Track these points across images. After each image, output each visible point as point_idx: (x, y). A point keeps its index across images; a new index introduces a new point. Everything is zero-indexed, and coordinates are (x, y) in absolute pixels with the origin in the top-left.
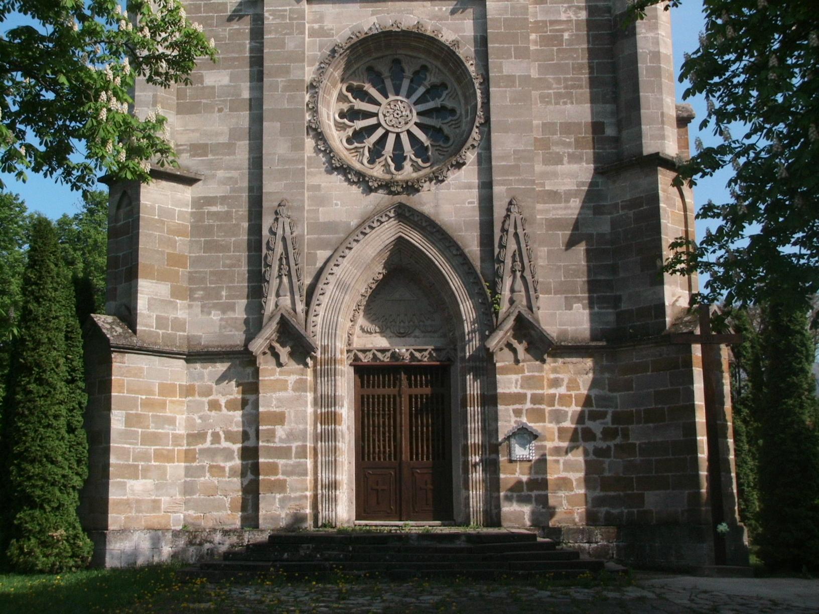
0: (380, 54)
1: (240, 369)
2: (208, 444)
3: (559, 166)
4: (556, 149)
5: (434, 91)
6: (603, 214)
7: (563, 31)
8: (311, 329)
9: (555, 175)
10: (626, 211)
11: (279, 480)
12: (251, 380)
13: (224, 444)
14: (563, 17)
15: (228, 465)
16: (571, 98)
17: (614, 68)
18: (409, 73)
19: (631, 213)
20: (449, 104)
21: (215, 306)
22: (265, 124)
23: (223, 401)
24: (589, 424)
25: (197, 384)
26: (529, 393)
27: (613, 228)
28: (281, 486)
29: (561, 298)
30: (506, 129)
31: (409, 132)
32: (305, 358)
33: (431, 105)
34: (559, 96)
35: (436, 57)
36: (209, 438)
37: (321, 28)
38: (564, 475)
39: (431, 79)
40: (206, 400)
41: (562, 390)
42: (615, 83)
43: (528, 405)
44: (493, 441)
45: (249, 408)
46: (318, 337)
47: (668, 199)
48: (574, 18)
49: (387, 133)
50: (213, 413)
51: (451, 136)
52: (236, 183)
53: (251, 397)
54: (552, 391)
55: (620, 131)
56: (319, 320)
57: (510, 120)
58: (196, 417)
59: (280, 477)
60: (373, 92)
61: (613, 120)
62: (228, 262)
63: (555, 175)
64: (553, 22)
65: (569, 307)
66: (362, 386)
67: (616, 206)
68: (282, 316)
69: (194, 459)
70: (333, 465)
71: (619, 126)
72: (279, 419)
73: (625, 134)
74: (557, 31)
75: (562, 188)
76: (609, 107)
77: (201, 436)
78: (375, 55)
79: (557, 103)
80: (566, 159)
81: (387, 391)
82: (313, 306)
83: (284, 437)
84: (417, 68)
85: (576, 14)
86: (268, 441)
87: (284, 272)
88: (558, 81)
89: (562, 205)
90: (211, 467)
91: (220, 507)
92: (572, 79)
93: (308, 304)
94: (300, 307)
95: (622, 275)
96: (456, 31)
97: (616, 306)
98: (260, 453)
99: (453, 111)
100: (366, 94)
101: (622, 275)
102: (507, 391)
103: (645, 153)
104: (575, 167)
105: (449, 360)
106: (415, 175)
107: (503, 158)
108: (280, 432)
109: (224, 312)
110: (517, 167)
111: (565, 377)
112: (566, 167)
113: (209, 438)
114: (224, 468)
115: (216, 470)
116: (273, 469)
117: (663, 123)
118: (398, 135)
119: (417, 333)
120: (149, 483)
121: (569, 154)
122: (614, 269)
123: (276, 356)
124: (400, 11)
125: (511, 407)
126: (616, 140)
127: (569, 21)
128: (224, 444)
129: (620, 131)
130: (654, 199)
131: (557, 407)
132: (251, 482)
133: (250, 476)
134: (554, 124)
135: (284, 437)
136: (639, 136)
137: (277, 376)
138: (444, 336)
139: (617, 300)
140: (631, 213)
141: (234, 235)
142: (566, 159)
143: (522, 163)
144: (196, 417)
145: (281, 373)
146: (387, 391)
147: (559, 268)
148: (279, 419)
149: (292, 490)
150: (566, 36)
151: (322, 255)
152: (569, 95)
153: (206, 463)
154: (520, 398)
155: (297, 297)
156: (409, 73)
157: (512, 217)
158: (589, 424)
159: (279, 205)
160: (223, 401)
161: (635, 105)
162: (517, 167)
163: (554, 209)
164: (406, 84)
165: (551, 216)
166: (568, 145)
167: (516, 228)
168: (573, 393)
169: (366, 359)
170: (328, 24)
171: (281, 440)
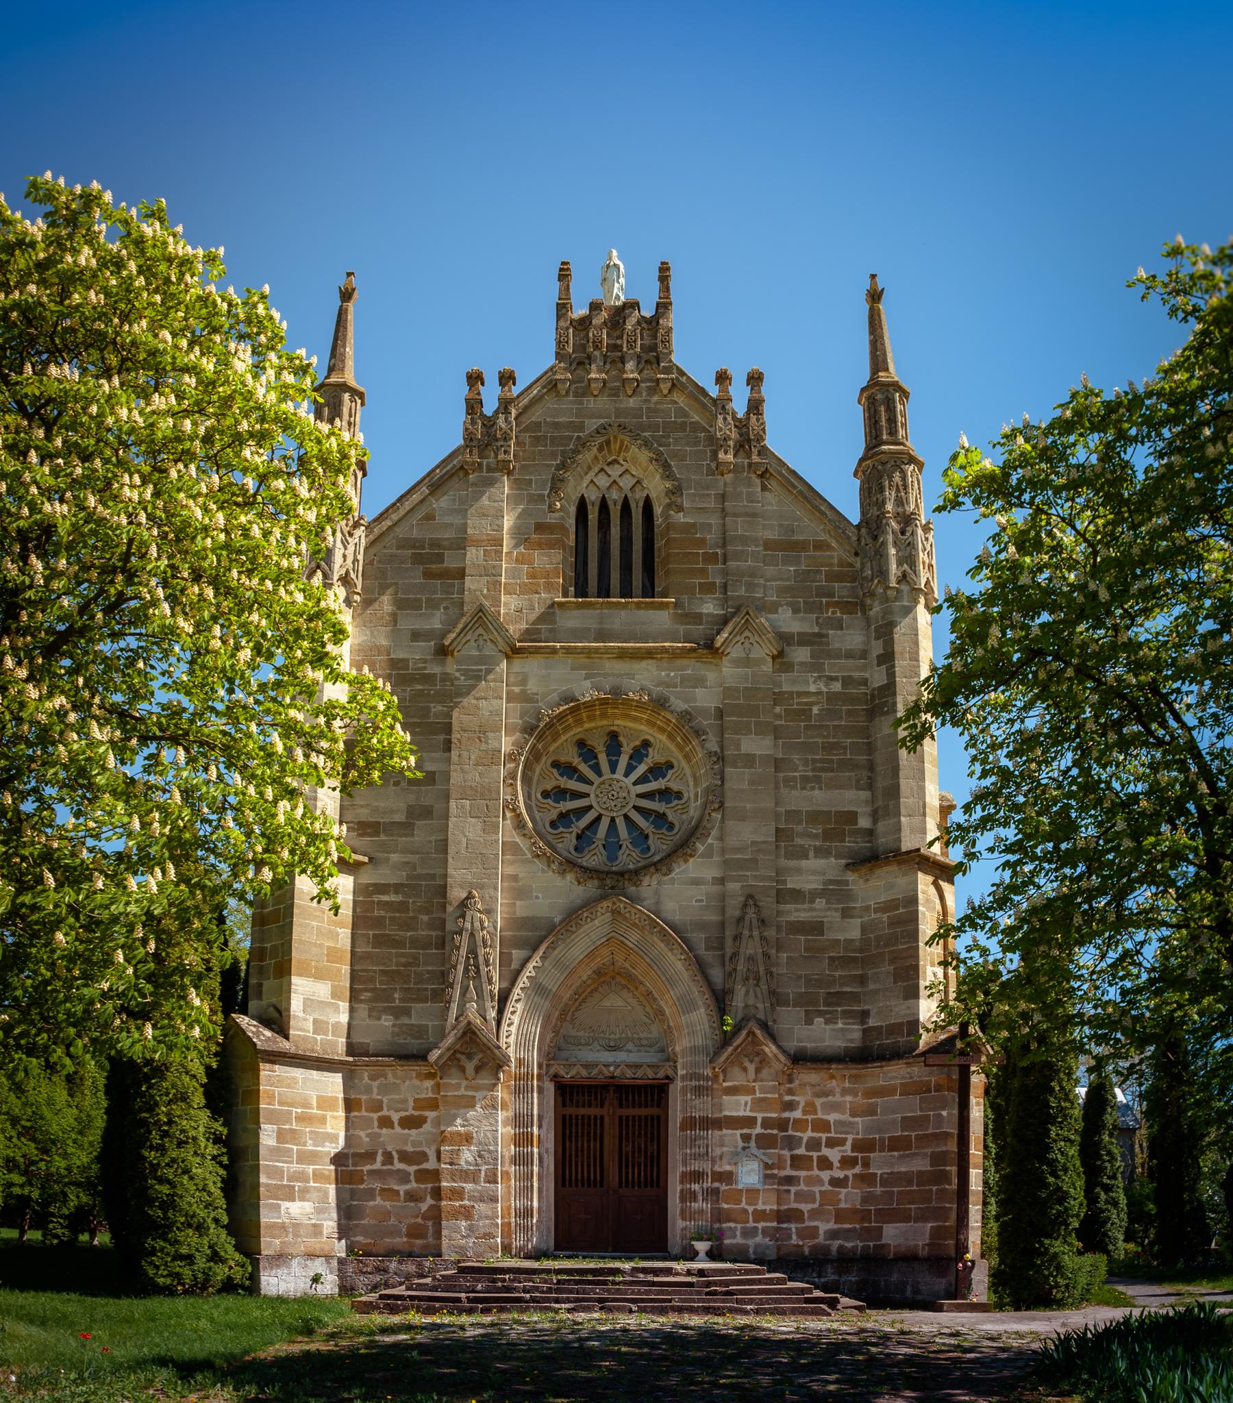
0: (593, 725)
1: (417, 1082)
2: (377, 1166)
3: (804, 863)
4: (798, 841)
5: (658, 771)
6: (852, 917)
7: (813, 704)
8: (503, 1040)
9: (799, 871)
10: (879, 915)
11: (464, 1207)
12: (430, 1095)
13: (398, 1165)
14: (812, 688)
15: (402, 1189)
16: (820, 782)
17: (870, 748)
18: (627, 750)
19: (885, 917)
20: (675, 787)
21: (386, 1010)
22: (453, 803)
23: (396, 1117)
24: (825, 1151)
25: (364, 1097)
26: (760, 1116)
27: (864, 929)
28: (467, 1213)
29: (800, 1012)
30: (742, 817)
31: (626, 816)
32: (497, 1074)
33: (653, 786)
34: (806, 780)
35: (662, 730)
36: (379, 1158)
37: (523, 692)
38: (794, 1206)
39: (654, 757)
40: (375, 1116)
41: (797, 1114)
42: (871, 767)
43: (758, 1130)
44: (717, 1168)
45: (427, 1127)
46: (512, 1049)
47: (928, 901)
48: (824, 689)
49: (599, 818)
50: (384, 1131)
51: (676, 822)
52: (415, 868)
53: (431, 1115)
54: (786, 1115)
55: (875, 822)
56: (513, 1029)
57: (748, 806)
58: (362, 1134)
59: (466, 1202)
60: (584, 768)
61: (868, 809)
62: (403, 960)
63: (799, 871)
64: (799, 694)
65: (809, 1022)
66: (564, 1105)
67: (868, 908)
68: (469, 1023)
69: (362, 1181)
70: (526, 1191)
71: (875, 816)
72: (467, 1139)
73: (881, 826)
74: (806, 704)
75: (808, 887)
76: (865, 795)
77: (370, 1156)
78: (587, 726)
79: (803, 788)
80: (811, 854)
81: (593, 1111)
82: (507, 1014)
83: (471, 1159)
84: (638, 743)
85: (827, 685)
86: (451, 1164)
87: (472, 974)
88: (806, 764)
89: (806, 906)
90: (383, 1190)
91: (394, 1232)
92: (822, 761)
93: (501, 1012)
94: (492, 1014)
95: (871, 987)
96: (686, 701)
97: (863, 1022)
98: (444, 1175)
99: (679, 795)
100: (575, 770)
101: (871, 987)
102: (734, 1114)
103: (904, 849)
104: (822, 863)
105: (667, 1077)
106: (631, 866)
107: (735, 850)
108: (467, 1155)
109: (397, 1018)
110: (755, 861)
111: (801, 1099)
112: (813, 863)
113: (379, 1158)
114: (398, 1192)
115: (390, 1194)
116: (458, 1194)
117: (924, 815)
118: (613, 819)
119: (630, 1046)
120: (308, 1207)
121: (816, 848)
122: (862, 980)
123: (462, 1070)
124: (619, 675)
125: (738, 1132)
126: (870, 833)
127: (819, 693)
128: (398, 1165)
129: (875, 822)
130: (913, 901)
131: (790, 1132)
132: (431, 1206)
133: (430, 1201)
134: (797, 812)
135: (471, 1159)
136: (898, 828)
137: (462, 1092)
138: (662, 1051)
139: (865, 1015)
140: (885, 917)
141: (413, 929)
142: (811, 854)
143: (761, 857)
144: (362, 1134)
145: (467, 1088)
146: (593, 1111)
147: (799, 977)
148: (467, 1139)
149: (480, 1218)
150: (815, 710)
151: (518, 955)
152: (818, 779)
153: (377, 1185)
154: (750, 1122)
155: (488, 1004)
156: (627, 750)
157: (747, 917)
158: (825, 1151)
159: (467, 898)
160: (396, 1117)
161: (894, 792)
162: (755, 861)
163: (797, 910)
164: (623, 761)
165: (792, 918)
166: (815, 836)
167: (751, 930)
168: (810, 1117)
169: (568, 1075)
170: (532, 687)
171: (467, 1163)
